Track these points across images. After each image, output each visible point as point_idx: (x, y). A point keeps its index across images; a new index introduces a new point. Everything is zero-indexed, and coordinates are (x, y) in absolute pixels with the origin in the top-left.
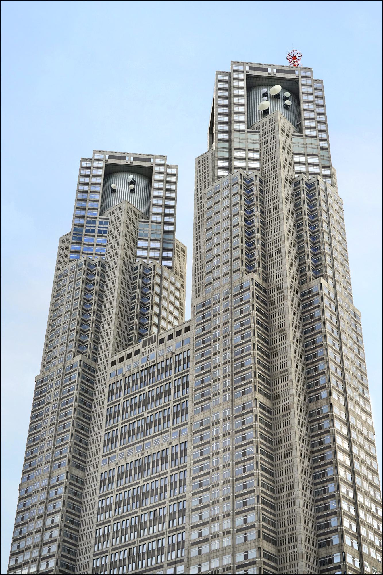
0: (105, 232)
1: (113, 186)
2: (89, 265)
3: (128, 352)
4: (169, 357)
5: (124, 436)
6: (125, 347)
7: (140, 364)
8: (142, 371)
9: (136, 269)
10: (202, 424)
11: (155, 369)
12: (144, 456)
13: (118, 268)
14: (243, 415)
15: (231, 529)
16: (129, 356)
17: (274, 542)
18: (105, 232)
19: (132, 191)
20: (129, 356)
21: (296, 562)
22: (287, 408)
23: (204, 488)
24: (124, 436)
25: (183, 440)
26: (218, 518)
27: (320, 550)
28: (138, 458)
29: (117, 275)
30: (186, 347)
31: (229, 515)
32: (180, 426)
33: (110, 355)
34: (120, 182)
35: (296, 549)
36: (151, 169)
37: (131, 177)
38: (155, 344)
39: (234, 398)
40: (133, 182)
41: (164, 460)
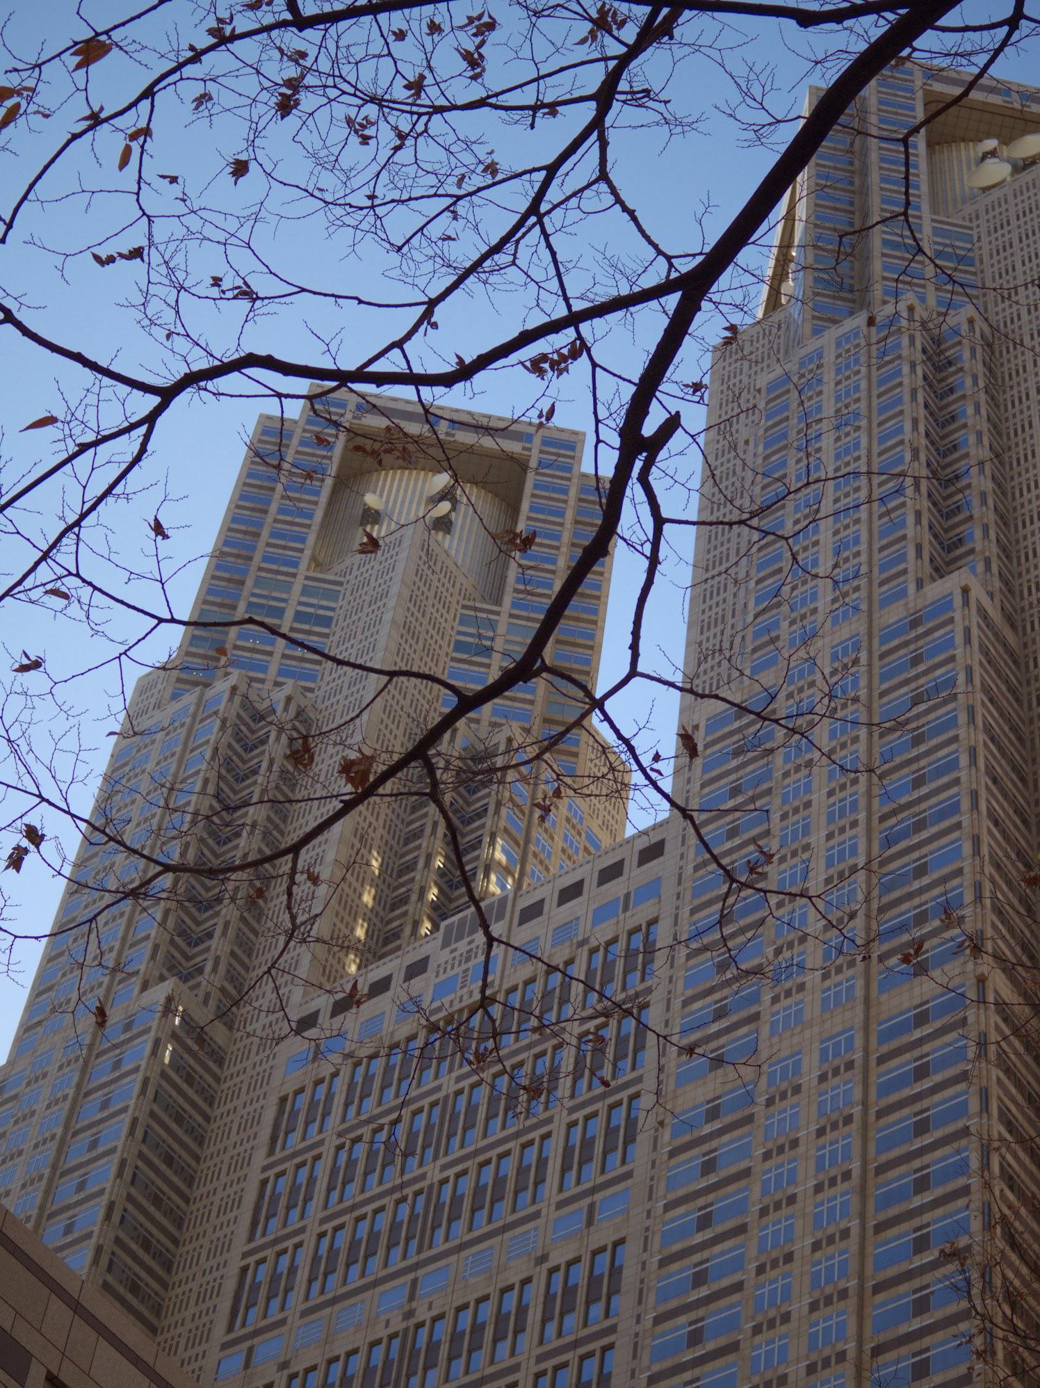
0: (327, 621)
1: (371, 500)
2: (247, 703)
5: (323, 1267)
12: (412, 1322)
18: (327, 621)
19: (444, 524)
23: (710, 1346)
24: (323, 1267)
25: (603, 1235)
28: (383, 1333)
30: (639, 915)
32: (593, 1191)
34: (400, 496)
36: (520, 465)
37: (442, 480)
39: (874, 993)
41: (509, 1325)
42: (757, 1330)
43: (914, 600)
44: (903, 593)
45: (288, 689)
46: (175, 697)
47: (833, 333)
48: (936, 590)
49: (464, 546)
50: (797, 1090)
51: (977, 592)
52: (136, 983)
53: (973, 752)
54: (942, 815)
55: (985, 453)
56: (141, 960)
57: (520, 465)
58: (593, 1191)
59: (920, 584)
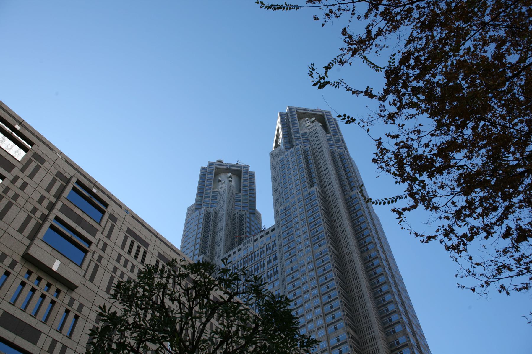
0: (216, 198)
1: (220, 178)
3: (234, 251)
4: (262, 247)
6: (232, 248)
7: (242, 255)
8: (244, 259)
9: (235, 214)
10: (292, 270)
11: (253, 255)
13: (225, 212)
14: (322, 257)
15: (324, 325)
16: (235, 253)
17: (355, 332)
18: (216, 198)
19: (230, 181)
20: (235, 253)
21: (375, 342)
22: (350, 253)
26: (312, 320)
27: (388, 337)
29: (224, 215)
30: (273, 239)
31: (321, 316)
32: (273, 282)
33: (222, 255)
34: (224, 178)
35: (373, 334)
36: (240, 171)
37: (230, 174)
38: (252, 243)
40: (230, 177)
42: (305, 303)
43: (309, 191)
44: (307, 190)
45: (213, 209)
46: (195, 211)
47: (289, 151)
48: (312, 189)
49: (234, 184)
50: (304, 265)
51: (318, 189)
52: (197, 256)
53: (322, 213)
54: (319, 223)
55: (315, 167)
56: (197, 252)
57: (240, 171)
58: (273, 282)
59: (309, 188)
